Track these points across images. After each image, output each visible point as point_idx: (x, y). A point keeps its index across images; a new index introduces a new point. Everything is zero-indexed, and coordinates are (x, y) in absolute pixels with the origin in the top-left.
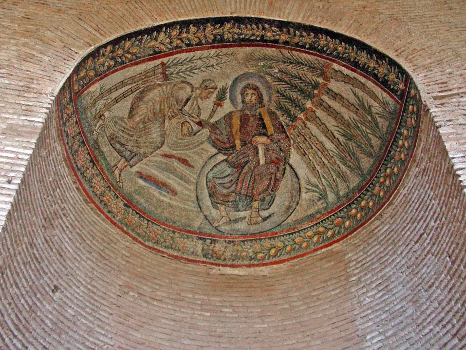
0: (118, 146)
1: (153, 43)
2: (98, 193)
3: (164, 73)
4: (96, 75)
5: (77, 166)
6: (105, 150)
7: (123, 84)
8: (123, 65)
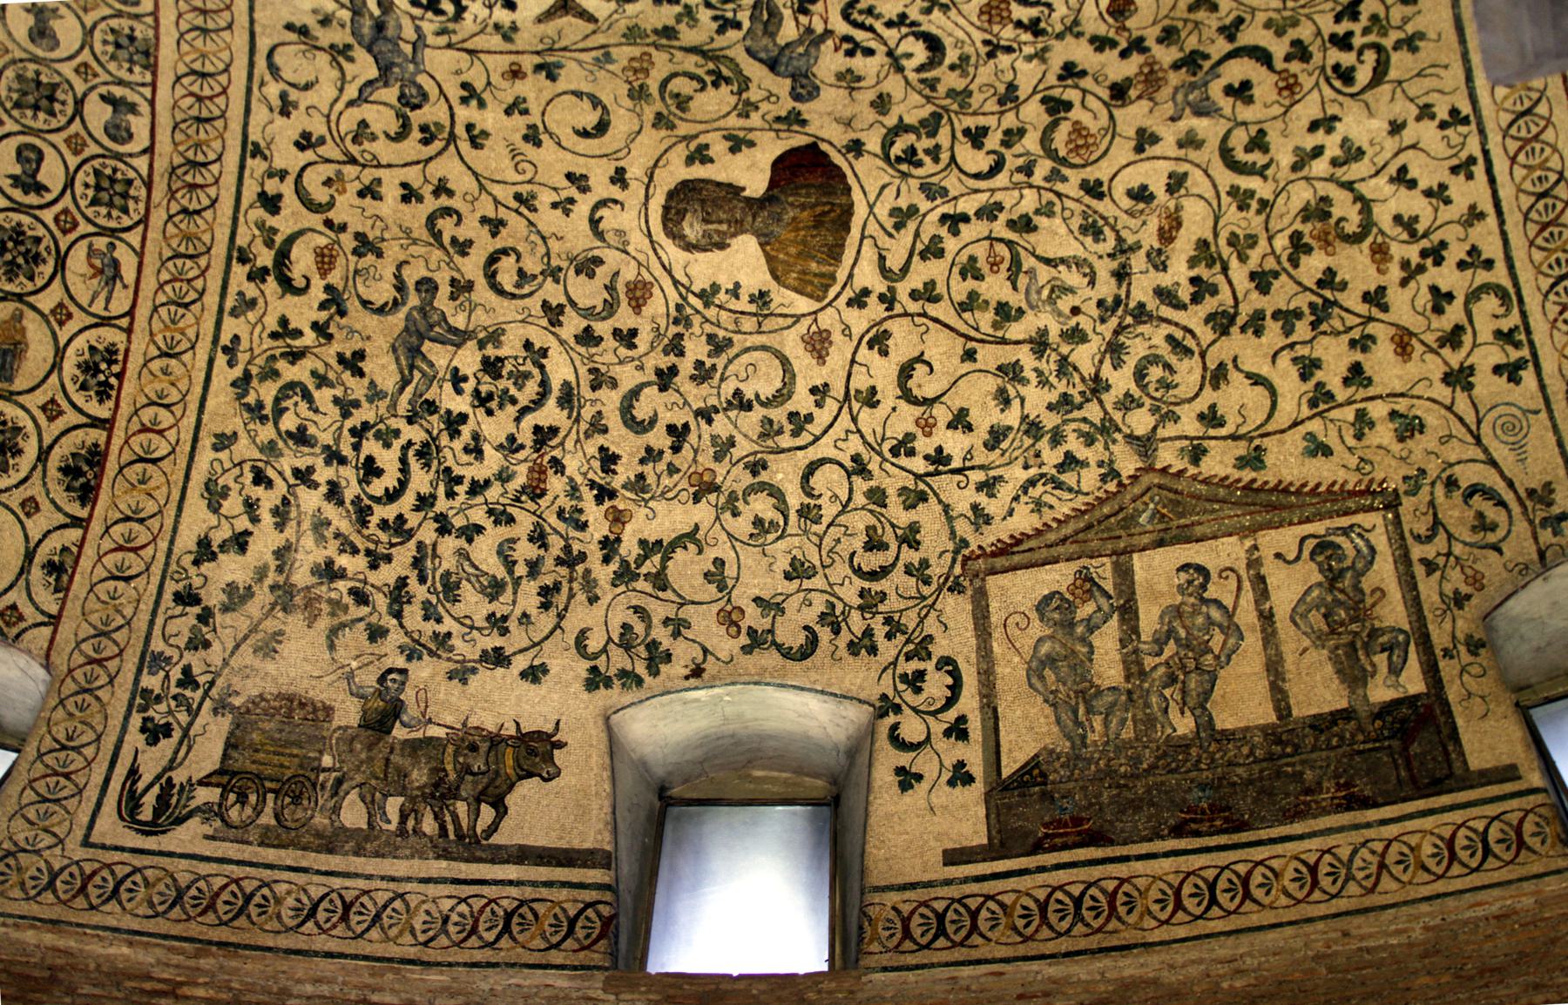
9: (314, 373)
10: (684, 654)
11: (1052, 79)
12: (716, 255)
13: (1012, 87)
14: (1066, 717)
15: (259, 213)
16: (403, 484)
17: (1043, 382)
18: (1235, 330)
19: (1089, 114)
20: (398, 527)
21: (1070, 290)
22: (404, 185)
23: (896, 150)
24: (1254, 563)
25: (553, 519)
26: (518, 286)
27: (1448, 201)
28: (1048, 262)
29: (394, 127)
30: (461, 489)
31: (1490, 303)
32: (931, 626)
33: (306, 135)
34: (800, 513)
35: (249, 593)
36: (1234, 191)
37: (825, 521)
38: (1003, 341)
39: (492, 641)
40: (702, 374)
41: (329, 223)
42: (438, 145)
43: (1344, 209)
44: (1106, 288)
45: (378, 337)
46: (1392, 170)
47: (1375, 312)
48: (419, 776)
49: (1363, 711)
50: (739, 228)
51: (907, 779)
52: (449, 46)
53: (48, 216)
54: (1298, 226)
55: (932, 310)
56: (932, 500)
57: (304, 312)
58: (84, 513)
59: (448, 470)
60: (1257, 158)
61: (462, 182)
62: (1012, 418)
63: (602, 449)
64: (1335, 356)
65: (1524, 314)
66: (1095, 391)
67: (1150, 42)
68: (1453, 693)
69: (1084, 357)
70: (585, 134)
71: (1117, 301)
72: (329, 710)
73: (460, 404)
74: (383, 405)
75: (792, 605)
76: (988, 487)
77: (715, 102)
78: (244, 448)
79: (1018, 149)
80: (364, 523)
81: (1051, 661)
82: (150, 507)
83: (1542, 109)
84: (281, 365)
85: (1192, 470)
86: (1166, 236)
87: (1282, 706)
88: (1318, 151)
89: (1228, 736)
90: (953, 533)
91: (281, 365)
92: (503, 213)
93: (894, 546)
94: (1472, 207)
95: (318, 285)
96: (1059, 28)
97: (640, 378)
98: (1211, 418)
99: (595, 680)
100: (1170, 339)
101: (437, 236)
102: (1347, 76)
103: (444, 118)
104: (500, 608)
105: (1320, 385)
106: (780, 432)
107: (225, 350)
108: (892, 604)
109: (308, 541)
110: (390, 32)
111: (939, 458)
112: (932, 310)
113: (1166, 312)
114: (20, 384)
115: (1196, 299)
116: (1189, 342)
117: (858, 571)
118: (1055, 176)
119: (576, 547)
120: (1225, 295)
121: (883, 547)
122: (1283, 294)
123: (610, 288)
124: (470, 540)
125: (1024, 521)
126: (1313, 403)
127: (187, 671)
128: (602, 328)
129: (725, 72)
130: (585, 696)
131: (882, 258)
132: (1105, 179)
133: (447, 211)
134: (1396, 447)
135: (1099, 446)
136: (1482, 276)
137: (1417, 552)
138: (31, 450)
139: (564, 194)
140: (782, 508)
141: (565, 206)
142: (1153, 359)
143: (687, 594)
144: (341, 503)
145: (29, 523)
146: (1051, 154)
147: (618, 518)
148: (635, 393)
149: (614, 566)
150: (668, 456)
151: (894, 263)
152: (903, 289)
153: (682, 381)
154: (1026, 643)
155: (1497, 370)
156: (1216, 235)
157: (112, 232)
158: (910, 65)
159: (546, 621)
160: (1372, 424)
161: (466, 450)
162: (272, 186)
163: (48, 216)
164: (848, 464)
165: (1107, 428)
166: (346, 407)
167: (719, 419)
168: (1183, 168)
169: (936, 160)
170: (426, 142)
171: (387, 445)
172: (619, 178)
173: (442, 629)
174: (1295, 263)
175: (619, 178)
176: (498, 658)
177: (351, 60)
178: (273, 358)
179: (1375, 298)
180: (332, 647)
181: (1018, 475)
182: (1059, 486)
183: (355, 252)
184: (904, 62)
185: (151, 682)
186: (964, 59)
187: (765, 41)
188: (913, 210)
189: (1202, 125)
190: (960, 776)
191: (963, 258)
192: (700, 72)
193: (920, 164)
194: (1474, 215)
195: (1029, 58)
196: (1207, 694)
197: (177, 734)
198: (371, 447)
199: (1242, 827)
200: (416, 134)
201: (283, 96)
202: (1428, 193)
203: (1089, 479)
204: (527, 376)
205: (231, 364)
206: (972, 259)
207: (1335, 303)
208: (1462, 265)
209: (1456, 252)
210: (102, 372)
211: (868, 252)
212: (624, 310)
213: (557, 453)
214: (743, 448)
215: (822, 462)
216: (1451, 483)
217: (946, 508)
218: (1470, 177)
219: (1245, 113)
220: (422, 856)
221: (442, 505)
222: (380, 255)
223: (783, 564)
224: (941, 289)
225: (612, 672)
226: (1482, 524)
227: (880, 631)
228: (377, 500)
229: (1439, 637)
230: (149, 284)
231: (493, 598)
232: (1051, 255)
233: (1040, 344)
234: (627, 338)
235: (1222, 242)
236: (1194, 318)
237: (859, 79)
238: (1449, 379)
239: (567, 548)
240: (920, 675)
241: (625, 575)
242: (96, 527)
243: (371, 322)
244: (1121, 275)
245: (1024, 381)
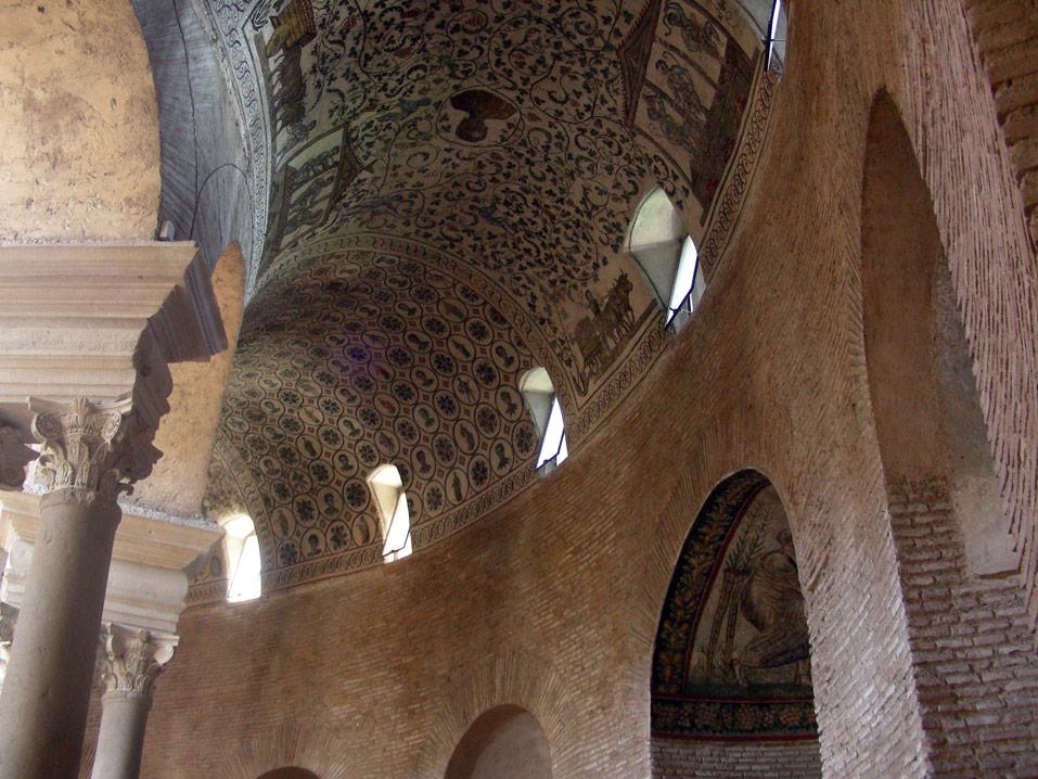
0: (781, 659)
1: (695, 573)
2: (797, 723)
3: (738, 573)
4: (683, 652)
5: (747, 731)
6: (768, 680)
7: (717, 623)
8: (696, 616)
10: (620, 219)
13: (442, 43)
16: (536, 246)
17: (573, 63)
20: (549, 257)
21: (539, 39)
23: (462, 76)
24: (665, 44)
32: (644, 151)
35: (549, 306)
38: (552, 67)
39: (591, 264)
44: (542, 27)
45: (484, 226)
55: (532, 81)
57: (470, 240)
62: (582, 80)
69: (567, 46)
72: (587, 318)
73: (516, 218)
74: (509, 236)
75: (619, 180)
76: (604, 101)
77: (423, 126)
78: (507, 277)
80: (543, 264)
82: (514, 310)
84: (485, 254)
85: (623, 38)
91: (485, 254)
98: (607, 20)
103: (408, 193)
111: (588, 108)
113: (559, 13)
116: (575, 11)
118: (489, 31)
125: (620, 100)
128: (505, 170)
131: (507, 88)
140: (587, 160)
141: (454, 166)
142: (577, 26)
146: (478, 31)
147: (571, 203)
148: (532, 173)
151: (510, 85)
152: (520, 86)
153: (532, 159)
154: (660, 132)
159: (592, 245)
165: (596, 53)
166: (505, 245)
176: (596, 266)
181: (603, 90)
182: (612, 81)
185: (558, 350)
192: (408, 130)
193: (471, 70)
203: (613, 70)
206: (516, 62)
210: (469, 294)
211: (504, 91)
214: (562, 155)
220: (627, 343)
221: (547, 242)
223: (606, 173)
230: (445, 270)
233: (557, 57)
234: (510, 166)
239: (574, 222)
244: (539, 21)
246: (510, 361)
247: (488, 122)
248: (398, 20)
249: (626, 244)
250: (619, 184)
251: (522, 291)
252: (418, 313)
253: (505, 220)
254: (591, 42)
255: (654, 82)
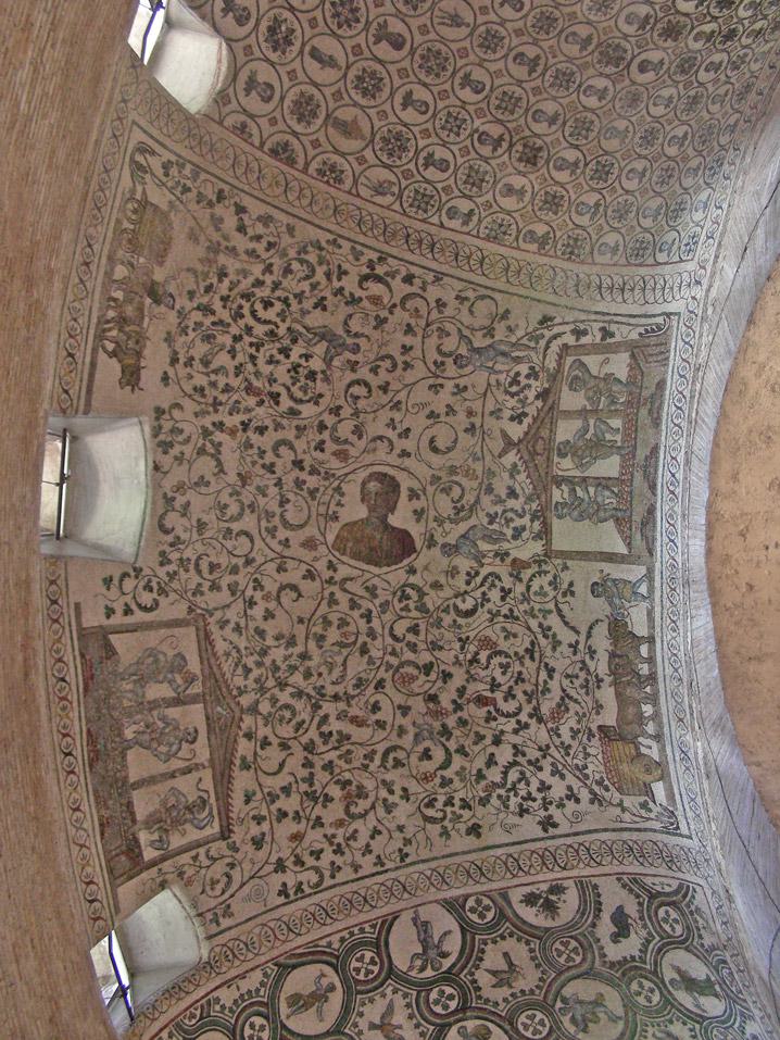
9: (318, 283)
11: (442, 667)
12: (358, 496)
13: (441, 648)
14: (132, 670)
15: (404, 273)
16: (258, 320)
17: (286, 658)
18: (306, 753)
19: (421, 684)
20: (239, 315)
21: (330, 673)
22: (411, 348)
23: (409, 591)
24: (197, 767)
25: (235, 397)
26: (352, 395)
27: (363, 855)
28: (345, 661)
29: (444, 348)
30: (253, 351)
31: (314, 878)
32: (173, 596)
33: (444, 305)
34: (228, 529)
35: (218, 229)
36: (374, 752)
37: (224, 542)
38: (307, 638)
40: (299, 483)
41: (394, 306)
42: (433, 368)
43: (363, 805)
44: (330, 690)
45: (332, 320)
46: (380, 828)
47: (311, 823)
48: (129, 311)
49: (136, 827)
50: (371, 510)
51: (108, 581)
52: (489, 384)
53: (412, 166)
54: (355, 783)
56: (232, 599)
57: (350, 284)
58: (266, 149)
59: (263, 345)
60: (391, 762)
61: (410, 377)
62: (270, 642)
63: (267, 427)
64: (291, 804)
65: (310, 895)
66: (280, 684)
67: (459, 714)
68: (144, 875)
69: (297, 678)
70: (432, 441)
71: (323, 695)
72: (161, 264)
74: (297, 316)
75: (184, 521)
76: (238, 629)
77: (445, 505)
78: (286, 240)
79: (405, 649)
80: (242, 297)
81: (157, 661)
82: (264, 185)
83: (406, 895)
84: (325, 268)
85: (241, 734)
86: (355, 721)
87: (137, 785)
88: (391, 792)
89: (124, 757)
90: (216, 609)
91: (325, 268)
92: (391, 394)
93: (211, 577)
94: (361, 867)
95: (363, 294)
96: (473, 672)
97: (299, 451)
99: (159, 412)
100: (304, 722)
101: (382, 358)
102: (430, 804)
104: (196, 363)
105: (278, 797)
106: (268, 521)
107: (335, 240)
108: (183, 575)
109: (238, 265)
110: (500, 358)
111: (251, 603)
112: (325, 602)
113: (317, 719)
114: (331, 130)
115: (322, 734)
117: (199, 558)
118: (389, 666)
119: (221, 408)
120: (323, 749)
121: (211, 573)
122: (322, 777)
123: (346, 441)
124: (229, 352)
125: (221, 647)
126: (269, 794)
127: (189, 190)
128: (326, 435)
129: (462, 514)
130: (152, 406)
131: (351, 579)
132: (385, 691)
133: (395, 366)
134: (249, 837)
135: (254, 686)
136: (327, 874)
137: (202, 851)
138: (299, 128)
139: (398, 426)
141: (392, 424)
142: (294, 714)
143: (195, 466)
144: (253, 286)
145: (265, 120)
146: (402, 665)
147: (233, 432)
148: (292, 448)
149: (211, 428)
150: (261, 462)
151: (348, 585)
154: (164, 648)
155: (284, 884)
156: (353, 744)
157: (400, 197)
158: (459, 602)
159: (188, 389)
160: (259, 824)
161: (272, 356)
162: (417, 281)
163: (412, 166)
164: (251, 556)
165: (262, 690)
166: (299, 296)
167: (276, 489)
168: (388, 728)
169: (402, 609)
170: (435, 363)
171: (278, 315)
172: (405, 454)
173: (190, 331)
174: (337, 782)
175: (405, 454)
176: (174, 361)
177: (484, 336)
178: (329, 264)
179: (319, 822)
180: (188, 270)
181: (242, 644)
182: (236, 665)
183: (377, 317)
184: (460, 598)
186: (460, 627)
187: (479, 535)
188: (375, 596)
189: (410, 737)
190: (110, 612)
191: (349, 620)
192: (464, 502)
193: (400, 601)
194: (356, 868)
195: (456, 657)
196: (141, 745)
197: (164, 179)
198: (278, 306)
199: (91, 766)
200: (440, 359)
201: (466, 299)
202: (368, 845)
203: (239, 681)
204: (305, 392)
205: (328, 241)
206: (348, 624)
207: (316, 803)
208: (333, 863)
209: (339, 860)
210: (331, 174)
211: (356, 573)
212: (335, 447)
213: (266, 404)
214: (262, 501)
215: (252, 541)
216: (232, 866)
217: (228, 606)
218: (375, 864)
219: (414, 759)
220: (100, 309)
221: (247, 339)
222: (375, 328)
223: (205, 518)
224: (335, 608)
225: (162, 422)
226: (214, 883)
227: (171, 568)
228: (252, 306)
229: (167, 866)
230: (372, 208)
231: (201, 360)
232: (348, 663)
233: (304, 656)
234: (320, 447)
235: (349, 747)
236: (313, 734)
237: (453, 577)
238: (280, 861)
239: (221, 404)
240: (151, 590)
241: (206, 433)
242: (259, 154)
243: (342, 318)
244: (336, 697)
245: (286, 648)
246: (251, 84)
247: (361, 512)
248: (499, 695)
249: (147, 429)
250: (184, 515)
251: (260, 229)
252: (398, 99)
253: (308, 342)
254: (274, 700)
255: (192, 706)
